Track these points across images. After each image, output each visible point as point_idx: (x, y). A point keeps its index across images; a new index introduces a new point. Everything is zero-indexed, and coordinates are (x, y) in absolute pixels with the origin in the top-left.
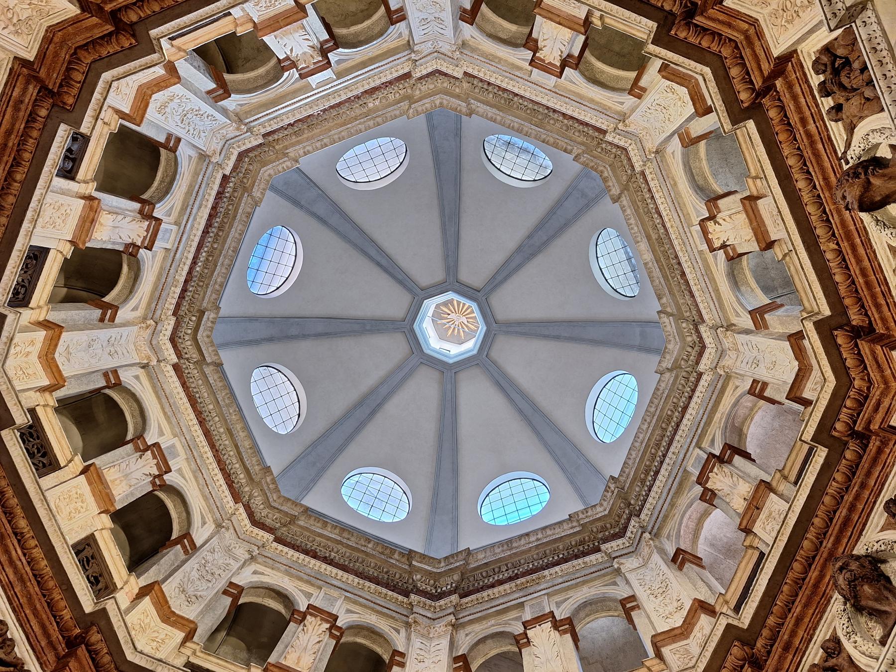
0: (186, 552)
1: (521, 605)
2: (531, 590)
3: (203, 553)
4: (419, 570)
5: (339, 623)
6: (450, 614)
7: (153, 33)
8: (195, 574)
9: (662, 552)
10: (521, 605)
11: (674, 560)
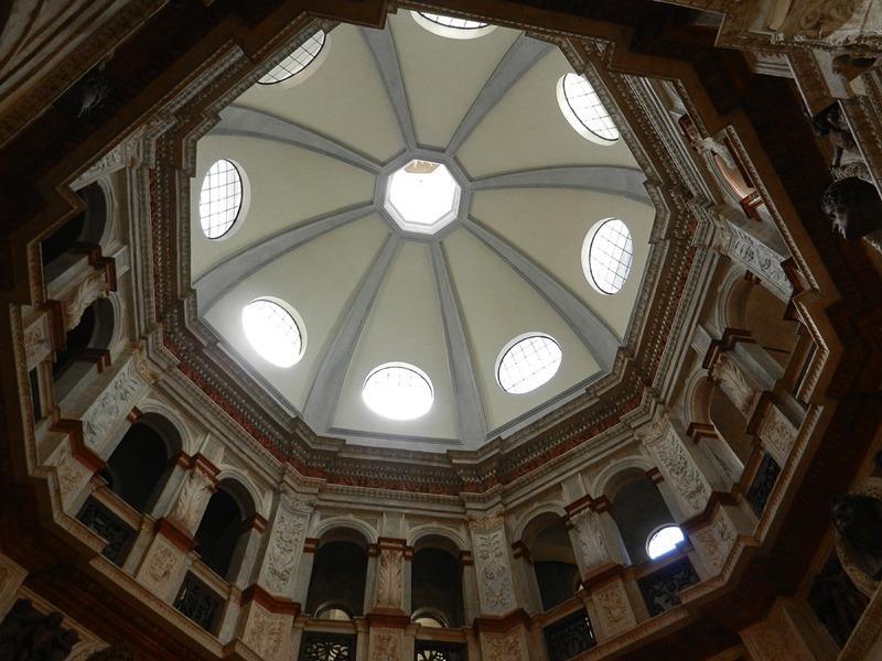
0: (261, 530)
1: (558, 487)
2: (564, 469)
3: (276, 526)
4: (460, 466)
7: (220, 655)
8: (277, 551)
9: (677, 424)
10: (558, 487)
11: (689, 432)
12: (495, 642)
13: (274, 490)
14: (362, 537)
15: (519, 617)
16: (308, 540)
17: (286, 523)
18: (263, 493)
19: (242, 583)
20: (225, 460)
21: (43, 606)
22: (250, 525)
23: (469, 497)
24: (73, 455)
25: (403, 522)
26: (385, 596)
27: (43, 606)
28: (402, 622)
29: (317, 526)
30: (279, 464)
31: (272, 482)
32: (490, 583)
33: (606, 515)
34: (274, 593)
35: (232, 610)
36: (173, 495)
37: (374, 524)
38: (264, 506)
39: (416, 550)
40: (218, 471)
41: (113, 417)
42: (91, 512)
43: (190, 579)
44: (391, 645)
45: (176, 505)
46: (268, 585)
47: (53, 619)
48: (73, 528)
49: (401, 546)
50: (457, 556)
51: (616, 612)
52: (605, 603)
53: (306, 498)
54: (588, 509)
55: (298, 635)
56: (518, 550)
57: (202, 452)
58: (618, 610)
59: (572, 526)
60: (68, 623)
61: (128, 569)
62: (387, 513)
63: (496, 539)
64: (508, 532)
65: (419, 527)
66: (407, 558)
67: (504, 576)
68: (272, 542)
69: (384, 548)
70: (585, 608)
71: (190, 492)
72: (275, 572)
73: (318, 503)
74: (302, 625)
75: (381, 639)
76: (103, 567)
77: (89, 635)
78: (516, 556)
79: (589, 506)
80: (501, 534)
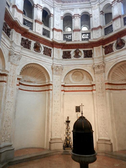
0: (52, 17)
3: (55, 15)
5: (80, 15)
6: (98, 2)
8: (56, 20)
12: (95, 32)
13: (53, 7)
14: (71, 14)
15: (100, 27)
16: (61, 17)
17: (57, 14)
18: (51, 9)
19: (52, 28)
20: (42, 3)
21: (25, 38)
22: (50, 16)
23: (92, 2)
24: (18, 12)
25: (78, 10)
26: (76, 26)
27: (25, 38)
28: (79, 30)
29: (62, 14)
30: (53, 1)
31: (52, 6)
32: (95, 21)
33: (120, 3)
34: (57, 28)
35: (51, 33)
36: (36, 14)
37: (73, 11)
38: (52, 12)
39: (81, 15)
40: (42, 7)
42: (25, 20)
43: (43, 29)
44: (78, 35)
45: (37, 16)
47: (27, 40)
49: (78, 15)
50: (89, 15)
51: (117, 25)
52: (116, 23)
53: (59, 8)
54: (116, 2)
55: (63, 35)
56: (101, 13)
57: (38, 3)
58: (118, 25)
59: (112, 7)
60: (29, 40)
61: (34, 30)
62: (75, 8)
63: (97, 11)
64: (99, 8)
65: (82, 10)
66: (79, 18)
67: (98, 19)
68: (55, 19)
69: (75, 16)
70: (112, 24)
72: (57, 25)
73: (62, 9)
75: (76, 34)
76: (30, 31)
78: (101, 14)
79: (117, 1)
80: (98, 10)
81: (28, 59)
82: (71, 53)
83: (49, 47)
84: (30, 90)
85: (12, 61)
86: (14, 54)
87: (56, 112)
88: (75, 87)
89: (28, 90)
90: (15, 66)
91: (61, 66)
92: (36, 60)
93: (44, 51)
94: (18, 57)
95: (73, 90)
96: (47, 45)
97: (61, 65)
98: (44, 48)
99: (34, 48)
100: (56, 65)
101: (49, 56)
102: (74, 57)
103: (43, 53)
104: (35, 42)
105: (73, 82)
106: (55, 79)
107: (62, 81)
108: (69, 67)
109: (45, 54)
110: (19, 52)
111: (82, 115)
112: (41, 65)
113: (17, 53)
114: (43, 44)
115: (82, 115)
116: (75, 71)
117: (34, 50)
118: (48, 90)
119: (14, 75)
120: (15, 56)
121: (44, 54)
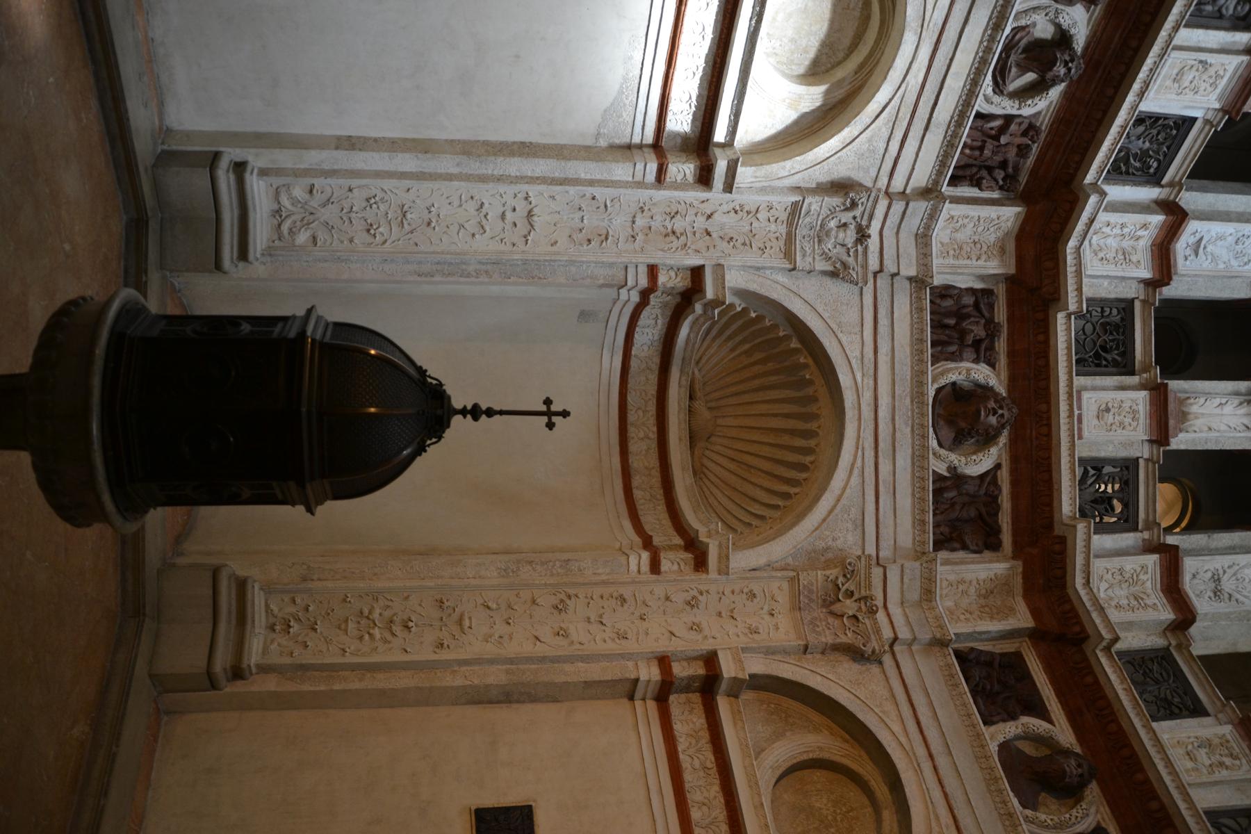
41: (1235, 263)
44: (1228, 761)
46: (1194, 576)
47: (990, 324)
48: (1074, 269)
60: (1001, 345)
71: (1228, 409)
74: (1174, 643)
77: (1004, 374)
81: (858, 346)
82: (1025, 719)
83: (1005, 520)
84: (633, 447)
85: (808, 213)
86: (864, 223)
87: (466, 623)
88: (715, 790)
89: (632, 431)
90: (782, 243)
91: (878, 631)
92: (867, 413)
93: (956, 479)
94: (851, 260)
95: (688, 777)
96: (1015, 497)
97: (887, 634)
98: (990, 477)
99: (954, 384)
100: (879, 602)
101: (936, 525)
102: (1004, 747)
103: (942, 469)
104: (1002, 391)
105: (766, 778)
106: (752, 596)
107: (757, 666)
108: (889, 707)
109: (937, 492)
110: (890, 267)
111: (464, 412)
112: (839, 456)
113: (873, 243)
114: (1014, 459)
115: (464, 412)
116: (867, 777)
117: (939, 391)
118: (647, 543)
119: (718, 242)
120: (850, 236)
121: (938, 478)
